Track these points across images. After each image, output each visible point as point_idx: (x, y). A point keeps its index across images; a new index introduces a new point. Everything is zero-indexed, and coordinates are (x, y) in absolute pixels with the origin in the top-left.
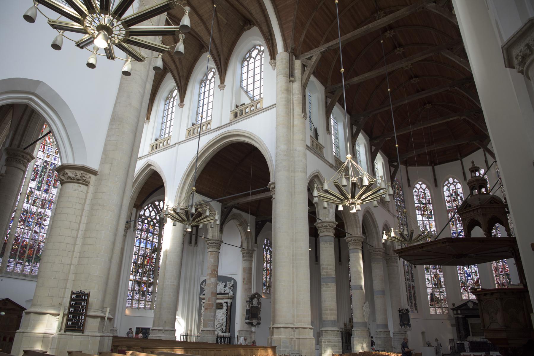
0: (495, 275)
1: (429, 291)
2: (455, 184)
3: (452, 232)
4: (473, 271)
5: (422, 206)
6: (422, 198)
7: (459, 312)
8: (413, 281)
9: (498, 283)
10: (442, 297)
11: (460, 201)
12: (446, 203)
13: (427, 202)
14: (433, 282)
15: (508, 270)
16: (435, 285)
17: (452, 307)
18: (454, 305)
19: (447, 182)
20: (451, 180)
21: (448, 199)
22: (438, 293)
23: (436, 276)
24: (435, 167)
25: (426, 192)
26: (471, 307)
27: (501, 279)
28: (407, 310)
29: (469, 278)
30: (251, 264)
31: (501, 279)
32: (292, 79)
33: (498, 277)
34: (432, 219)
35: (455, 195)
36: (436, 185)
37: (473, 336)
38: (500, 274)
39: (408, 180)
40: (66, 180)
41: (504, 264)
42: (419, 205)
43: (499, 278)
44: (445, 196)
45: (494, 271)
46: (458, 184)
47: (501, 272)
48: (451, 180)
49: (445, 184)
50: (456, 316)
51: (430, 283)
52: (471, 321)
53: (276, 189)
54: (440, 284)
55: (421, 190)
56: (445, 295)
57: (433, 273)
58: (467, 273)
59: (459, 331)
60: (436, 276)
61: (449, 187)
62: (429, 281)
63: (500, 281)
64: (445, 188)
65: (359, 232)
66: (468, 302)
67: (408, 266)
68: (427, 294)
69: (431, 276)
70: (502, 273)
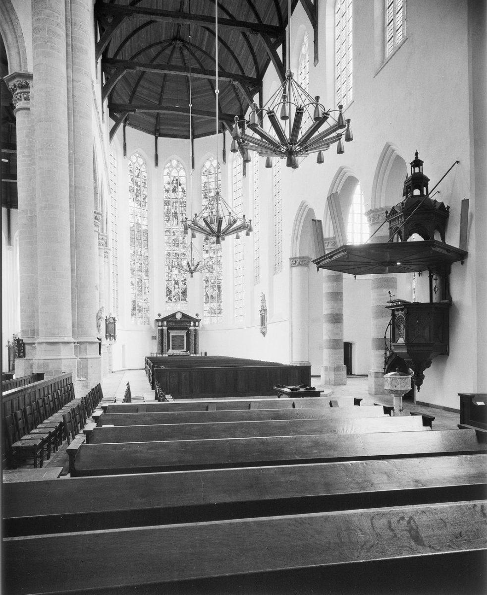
0: (205, 286)
2: (178, 169)
3: (166, 229)
4: (183, 279)
5: (136, 187)
6: (137, 177)
7: (165, 323)
9: (207, 294)
12: (165, 191)
13: (142, 184)
17: (157, 318)
18: (159, 315)
19: (169, 164)
20: (174, 162)
21: (167, 187)
22: (141, 301)
24: (159, 138)
25: (142, 169)
26: (179, 319)
29: (177, 286)
34: (145, 208)
35: (177, 184)
36: (157, 164)
39: (125, 145)
42: (132, 185)
44: (164, 182)
46: (182, 170)
48: (174, 162)
49: (166, 166)
50: (160, 328)
52: (173, 333)
53: (31, 90)
55: (136, 165)
57: (139, 276)
58: (174, 280)
61: (171, 171)
64: (166, 171)
66: (177, 313)
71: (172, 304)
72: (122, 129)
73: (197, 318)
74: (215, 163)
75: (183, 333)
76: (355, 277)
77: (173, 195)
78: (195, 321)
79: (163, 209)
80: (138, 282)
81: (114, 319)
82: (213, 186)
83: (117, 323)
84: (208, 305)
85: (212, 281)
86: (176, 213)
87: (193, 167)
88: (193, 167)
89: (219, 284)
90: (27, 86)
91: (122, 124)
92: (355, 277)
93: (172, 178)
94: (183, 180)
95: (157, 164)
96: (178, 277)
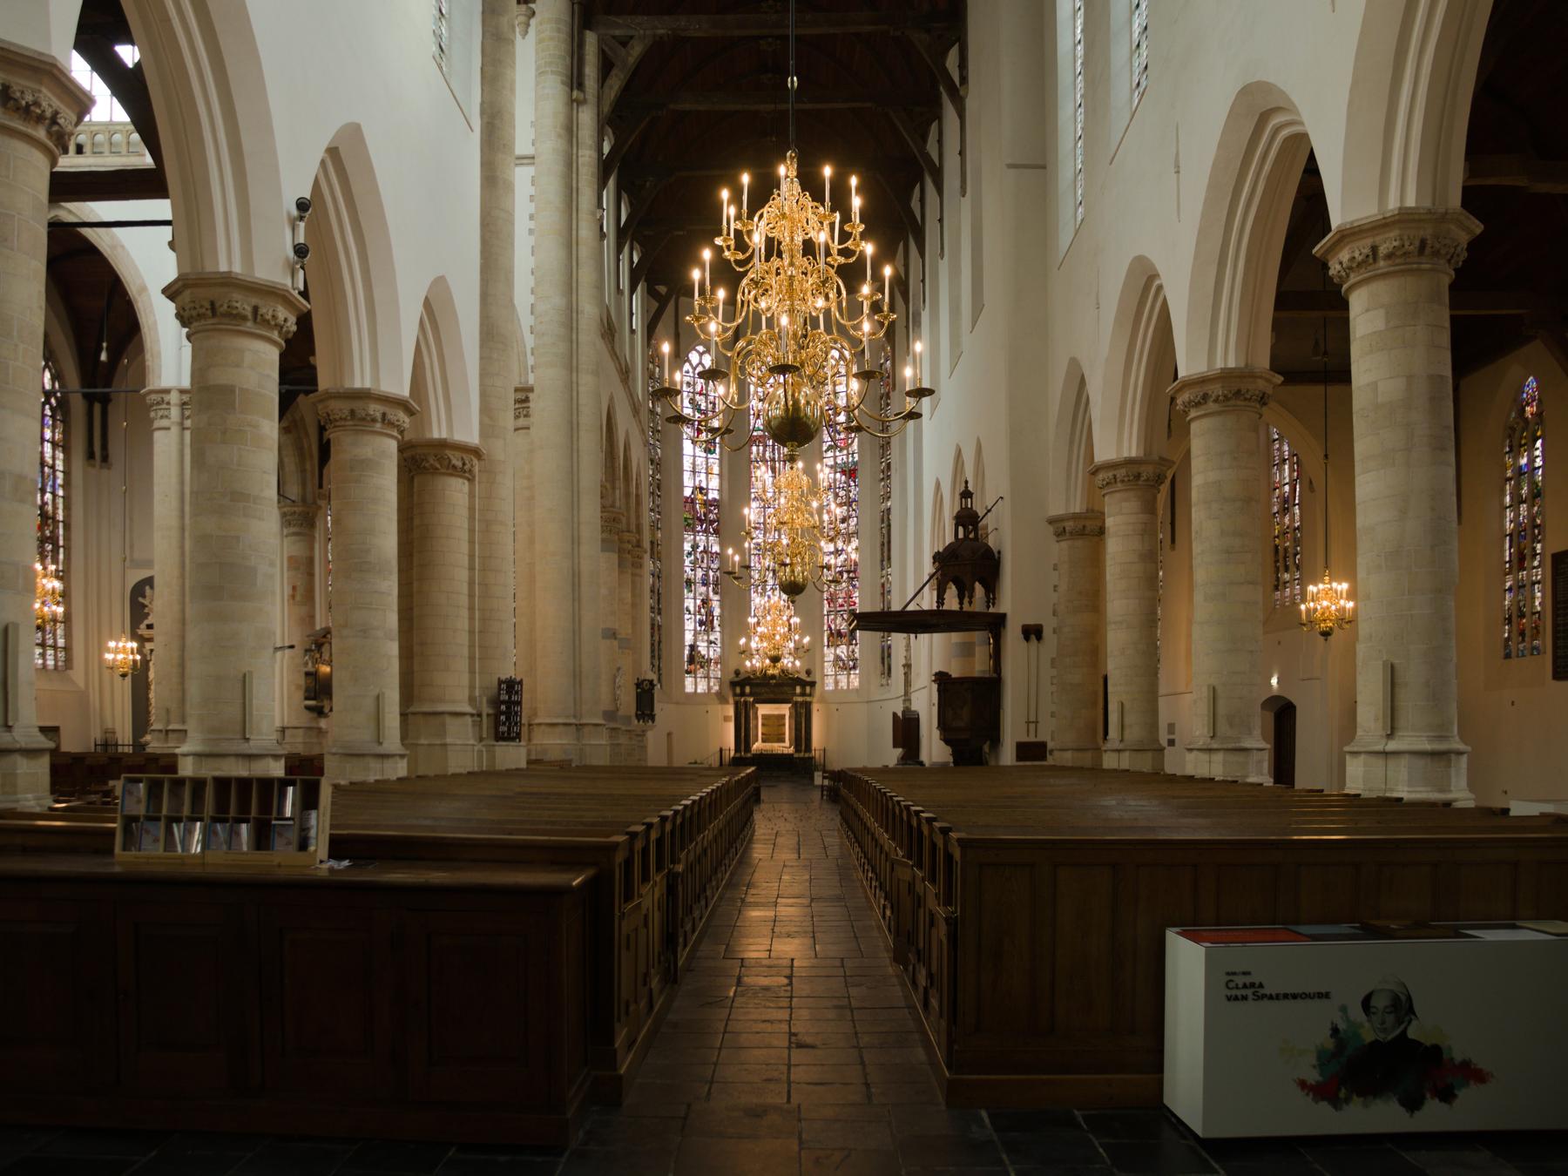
1: (689, 638)
8: (659, 614)
9: (829, 627)
10: (711, 653)
14: (698, 617)
15: (855, 603)
16: (700, 626)
17: (732, 676)
22: (706, 644)
23: (706, 603)
27: (839, 620)
30: (312, 549)
31: (838, 622)
33: (832, 617)
38: (838, 609)
40: (442, 471)
41: (851, 588)
43: (835, 619)
45: (826, 602)
47: (842, 606)
51: (691, 618)
54: (712, 621)
56: (719, 650)
57: (701, 594)
60: (705, 602)
62: (690, 613)
63: (836, 626)
65: (618, 501)
67: (653, 575)
68: (683, 646)
69: (695, 603)
70: (842, 608)
73: (808, 679)
76: (916, 637)
78: (803, 684)
80: (700, 608)
84: (832, 650)
85: (840, 601)
89: (853, 607)
92: (916, 637)
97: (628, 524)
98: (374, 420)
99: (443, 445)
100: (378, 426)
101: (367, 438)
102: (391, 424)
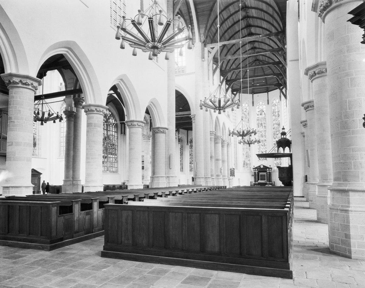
2: (262, 105)
5: (244, 116)
7: (256, 170)
11: (264, 115)
13: (247, 114)
18: (254, 166)
19: (258, 104)
20: (261, 103)
21: (258, 113)
24: (254, 95)
25: (247, 108)
28: (234, 169)
32: (203, 60)
36: (253, 105)
37: (261, 180)
52: (261, 174)
59: (255, 178)
64: (258, 107)
71: (261, 161)
72: (238, 95)
74: (277, 101)
75: (265, 173)
77: (260, 116)
78: (269, 168)
79: (256, 122)
81: (234, 169)
82: (277, 111)
83: (235, 170)
86: (262, 124)
87: (268, 104)
88: (268, 104)
90: (194, 117)
91: (238, 94)
93: (260, 109)
94: (264, 110)
95: (253, 105)
96: (263, 150)
97: (226, 138)
98: (135, 125)
99: (158, 128)
100: (137, 126)
101: (133, 128)
102: (139, 126)
